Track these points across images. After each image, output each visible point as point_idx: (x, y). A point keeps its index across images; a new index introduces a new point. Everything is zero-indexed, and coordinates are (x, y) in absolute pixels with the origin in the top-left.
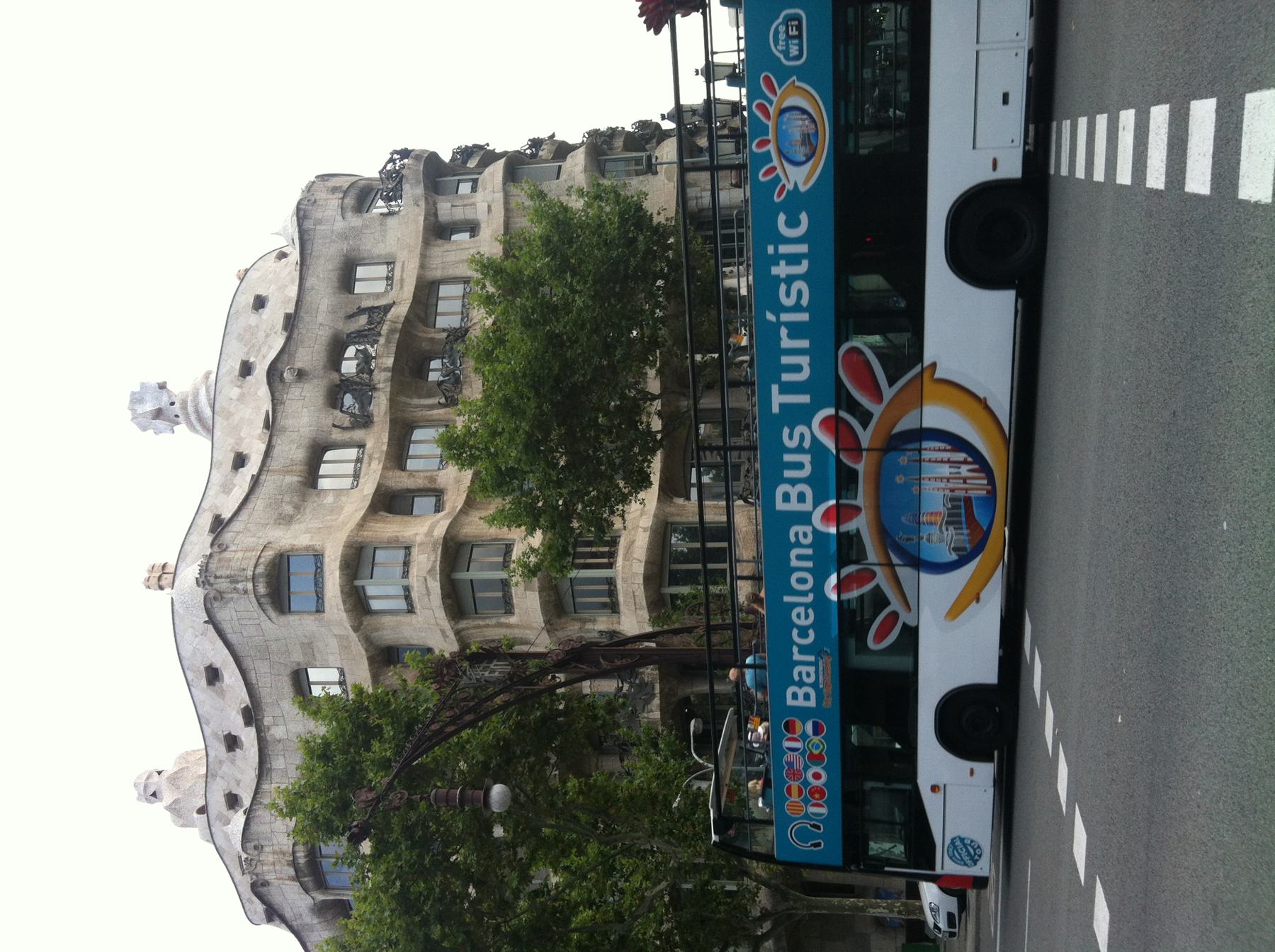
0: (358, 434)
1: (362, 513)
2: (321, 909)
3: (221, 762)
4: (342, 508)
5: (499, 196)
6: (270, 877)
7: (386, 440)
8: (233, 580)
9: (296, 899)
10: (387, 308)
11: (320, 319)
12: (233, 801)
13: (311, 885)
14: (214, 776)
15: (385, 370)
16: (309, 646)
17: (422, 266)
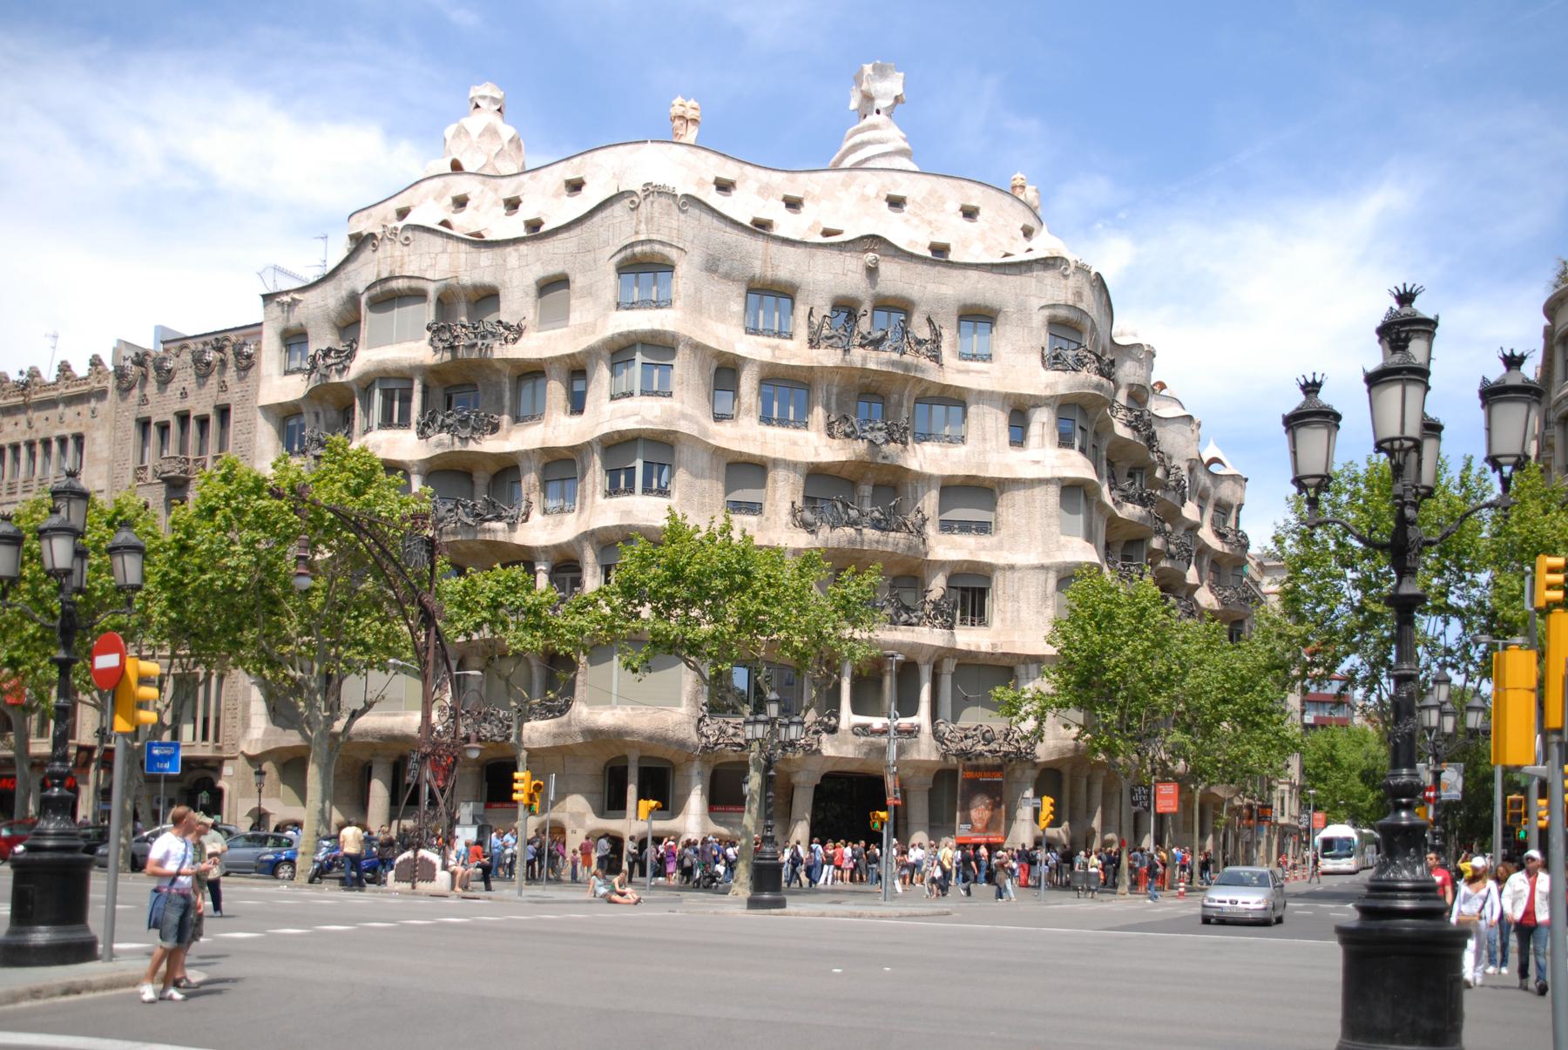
0: (802, 333)
1: (713, 344)
2: (354, 298)
3: (496, 190)
4: (723, 321)
5: (1047, 474)
6: (380, 253)
7: (793, 363)
8: (650, 220)
9: (363, 275)
10: (936, 358)
11: (931, 287)
12: (461, 202)
13: (375, 291)
14: (484, 183)
15: (864, 359)
16: (589, 292)
17: (980, 393)
